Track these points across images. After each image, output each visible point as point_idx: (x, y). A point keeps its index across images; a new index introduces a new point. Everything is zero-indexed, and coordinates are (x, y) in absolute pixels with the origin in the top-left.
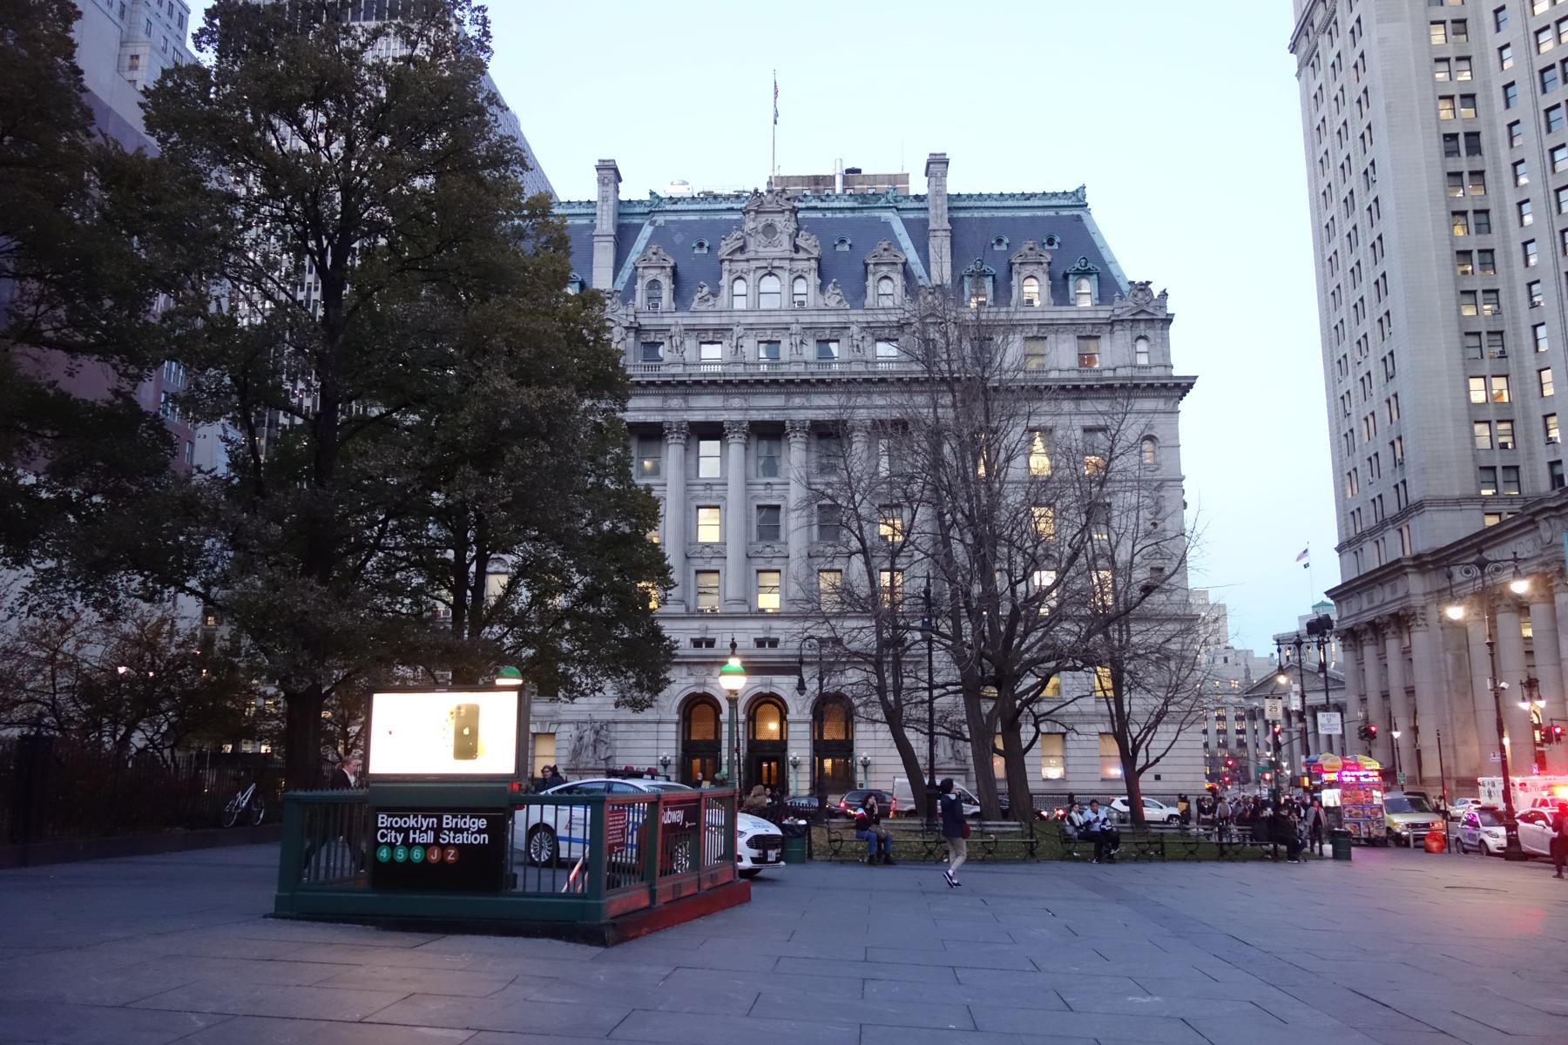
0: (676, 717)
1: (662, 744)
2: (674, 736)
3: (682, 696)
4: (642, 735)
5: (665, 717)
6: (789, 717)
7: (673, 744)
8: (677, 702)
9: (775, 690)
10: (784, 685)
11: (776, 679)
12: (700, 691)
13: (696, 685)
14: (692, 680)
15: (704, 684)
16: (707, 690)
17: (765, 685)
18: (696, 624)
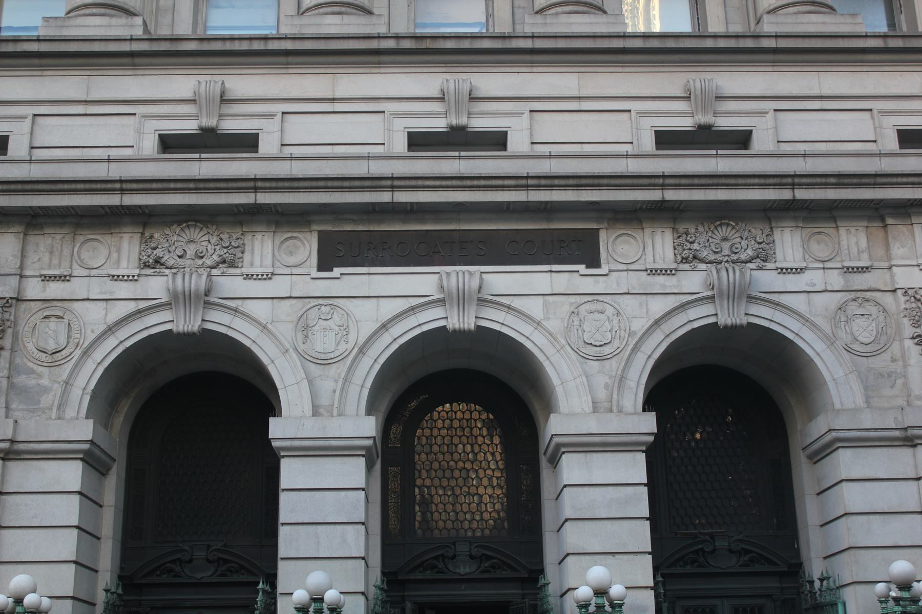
0: (83, 430)
1: (17, 544)
2: (69, 510)
3: (110, 349)
5: (34, 429)
6: (556, 426)
7: (66, 545)
8: (90, 374)
9: (496, 320)
10: (529, 303)
11: (502, 279)
12: (186, 322)
13: (179, 300)
14: (156, 286)
15: (205, 299)
16: (220, 321)
17: (461, 299)
18: (181, 84)
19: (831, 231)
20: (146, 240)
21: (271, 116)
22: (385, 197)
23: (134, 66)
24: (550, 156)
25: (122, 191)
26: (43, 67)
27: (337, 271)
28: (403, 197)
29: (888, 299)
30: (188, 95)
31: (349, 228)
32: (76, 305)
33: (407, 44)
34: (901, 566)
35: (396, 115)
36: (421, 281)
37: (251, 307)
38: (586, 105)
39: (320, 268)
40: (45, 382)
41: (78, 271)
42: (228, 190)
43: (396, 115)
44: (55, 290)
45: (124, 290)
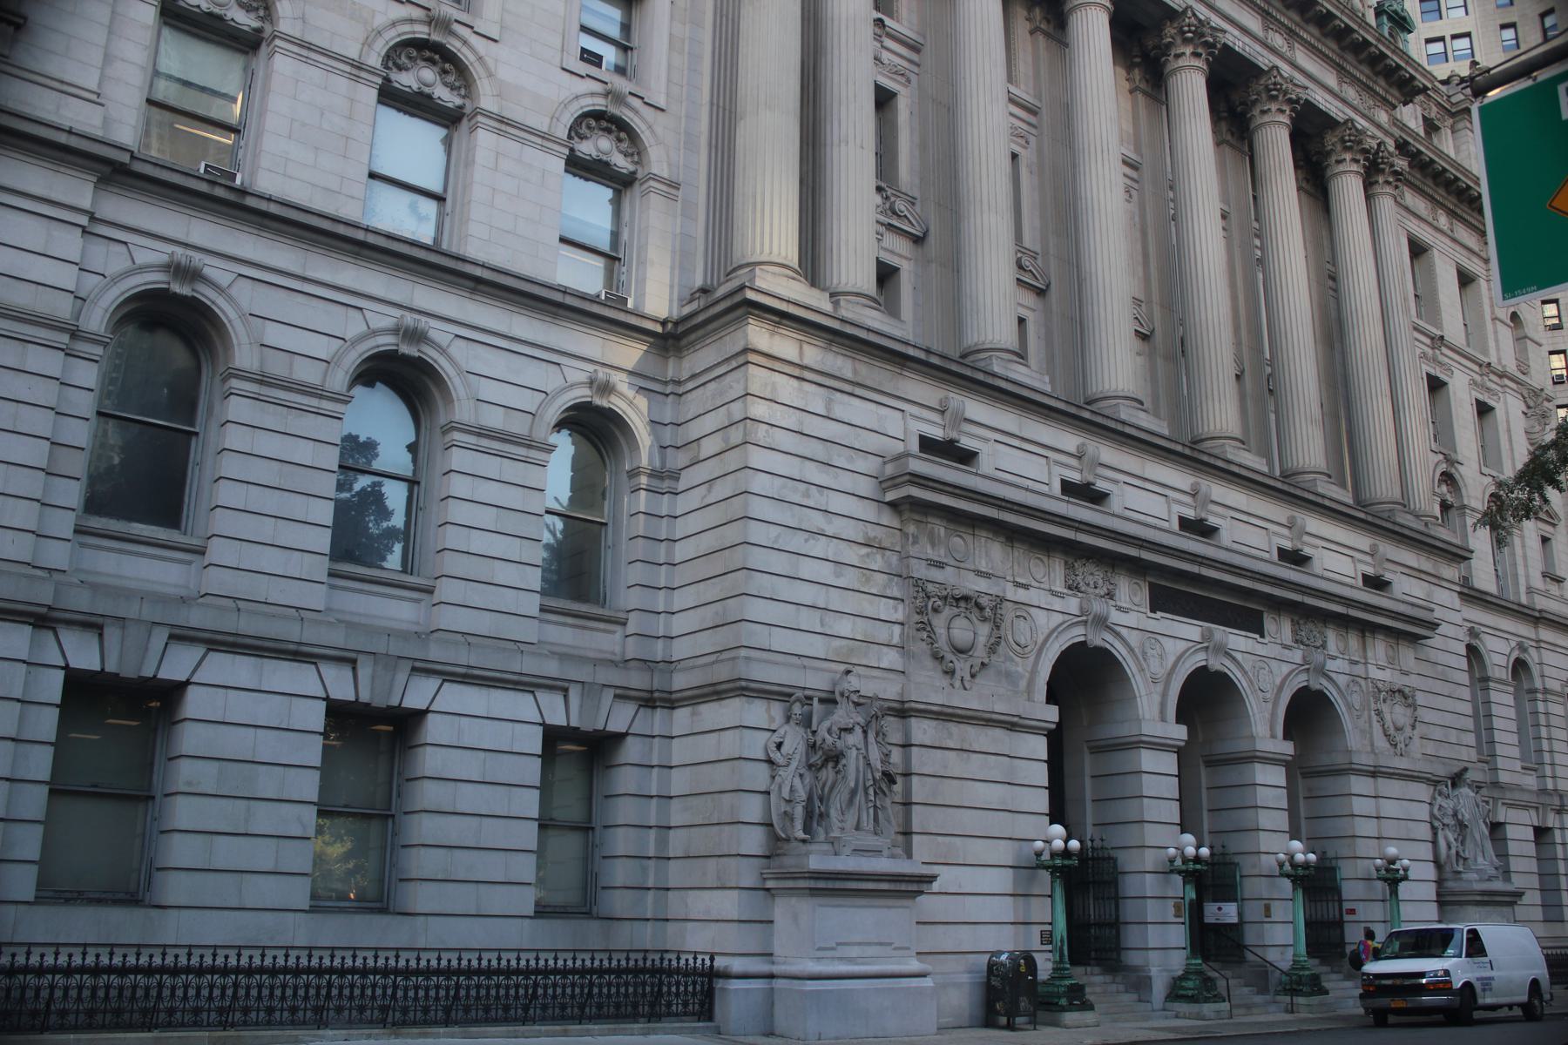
4: (974, 766)
19: (1045, 559)
20: (1069, 567)
21: (1116, 482)
22: (1194, 569)
23: (1047, 417)
24: (1027, 489)
25: (1077, 530)
26: (997, 399)
27: (1159, 614)
28: (1206, 572)
29: (1363, 682)
30: (1073, 450)
31: (1163, 583)
32: (1032, 610)
33: (935, 360)
34: (1392, 850)
35: (1057, 463)
36: (1191, 630)
37: (1124, 632)
38: (1253, 520)
39: (1153, 610)
40: (1020, 669)
41: (1034, 583)
42: (1179, 558)
43: (1275, 533)
44: (1021, 595)
45: (1057, 604)
